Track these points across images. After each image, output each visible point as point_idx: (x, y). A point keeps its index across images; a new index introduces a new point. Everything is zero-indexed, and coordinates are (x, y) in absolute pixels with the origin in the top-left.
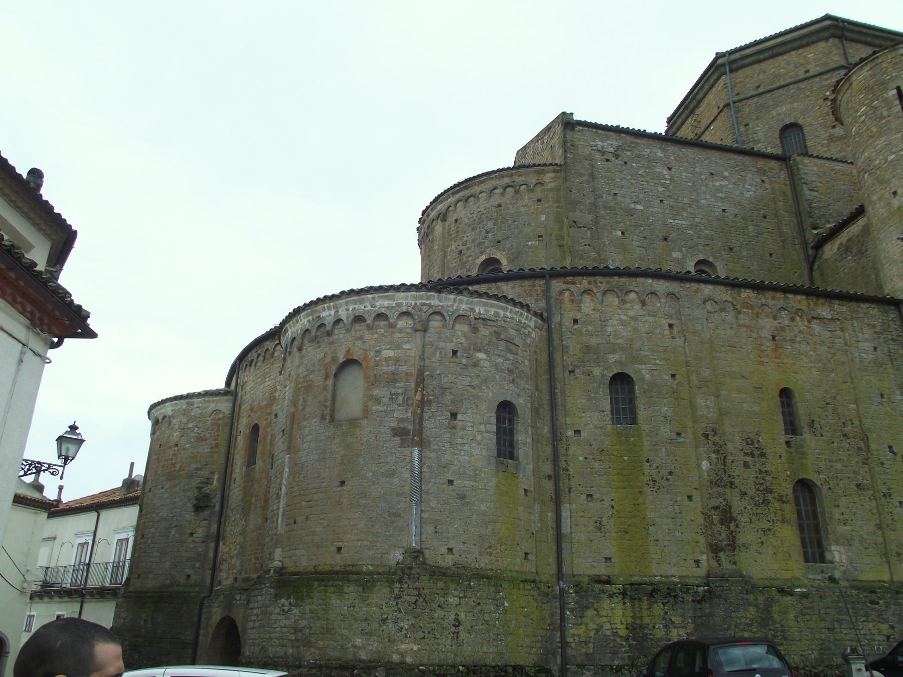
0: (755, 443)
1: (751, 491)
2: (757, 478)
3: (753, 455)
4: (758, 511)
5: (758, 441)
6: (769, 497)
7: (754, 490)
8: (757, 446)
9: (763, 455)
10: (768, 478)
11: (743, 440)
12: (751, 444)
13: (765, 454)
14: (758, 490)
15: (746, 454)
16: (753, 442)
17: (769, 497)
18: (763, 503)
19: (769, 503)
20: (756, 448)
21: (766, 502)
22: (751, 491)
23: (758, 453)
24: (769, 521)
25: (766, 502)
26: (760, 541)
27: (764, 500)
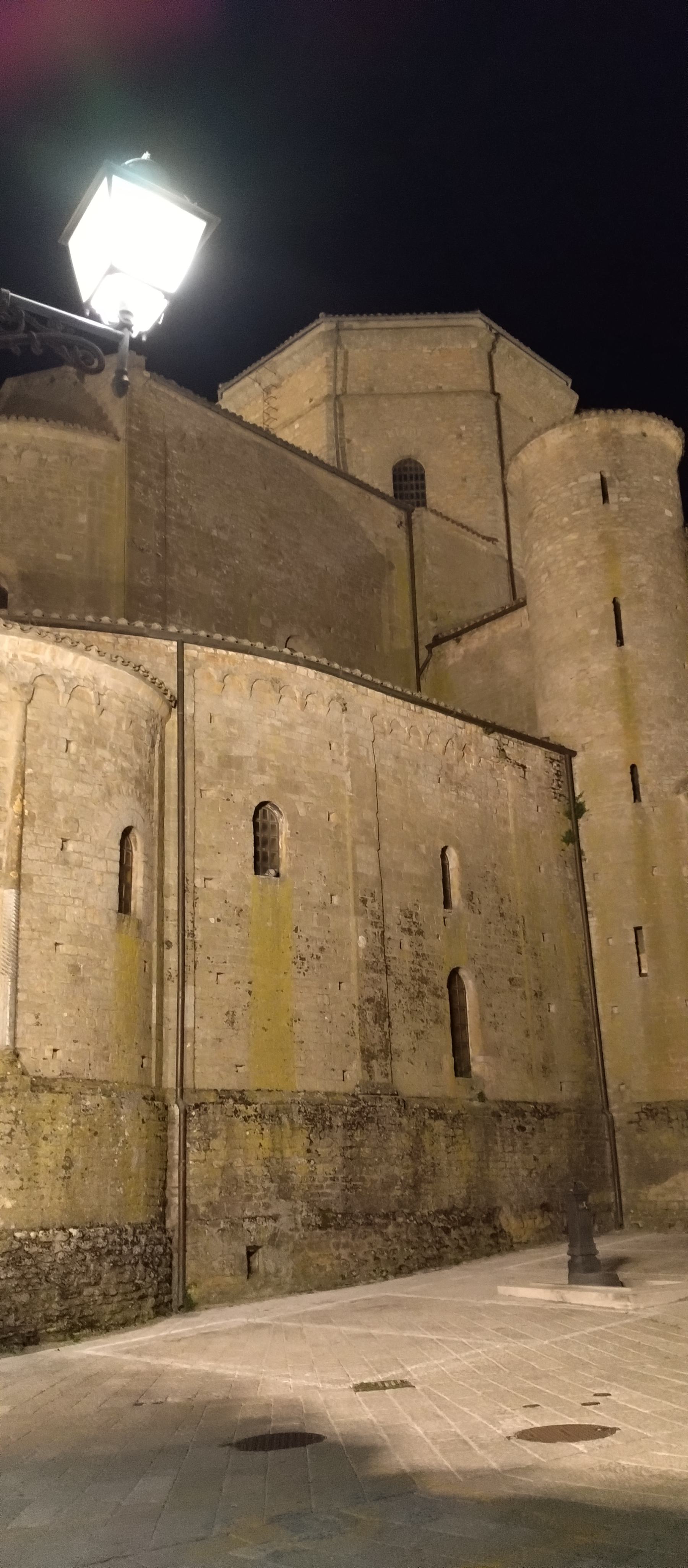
0: (414, 916)
1: (407, 980)
2: (413, 962)
3: (409, 931)
4: (412, 1007)
5: (417, 914)
6: (425, 989)
7: (409, 978)
8: (415, 920)
9: (420, 933)
10: (425, 964)
11: (401, 911)
12: (409, 918)
13: (423, 932)
14: (413, 978)
15: (403, 930)
16: (412, 915)
17: (425, 989)
18: (418, 997)
19: (423, 997)
20: (414, 923)
21: (420, 995)
22: (407, 980)
23: (416, 929)
24: (423, 1021)
25: (421, 995)
26: (412, 1047)
27: (420, 992)
